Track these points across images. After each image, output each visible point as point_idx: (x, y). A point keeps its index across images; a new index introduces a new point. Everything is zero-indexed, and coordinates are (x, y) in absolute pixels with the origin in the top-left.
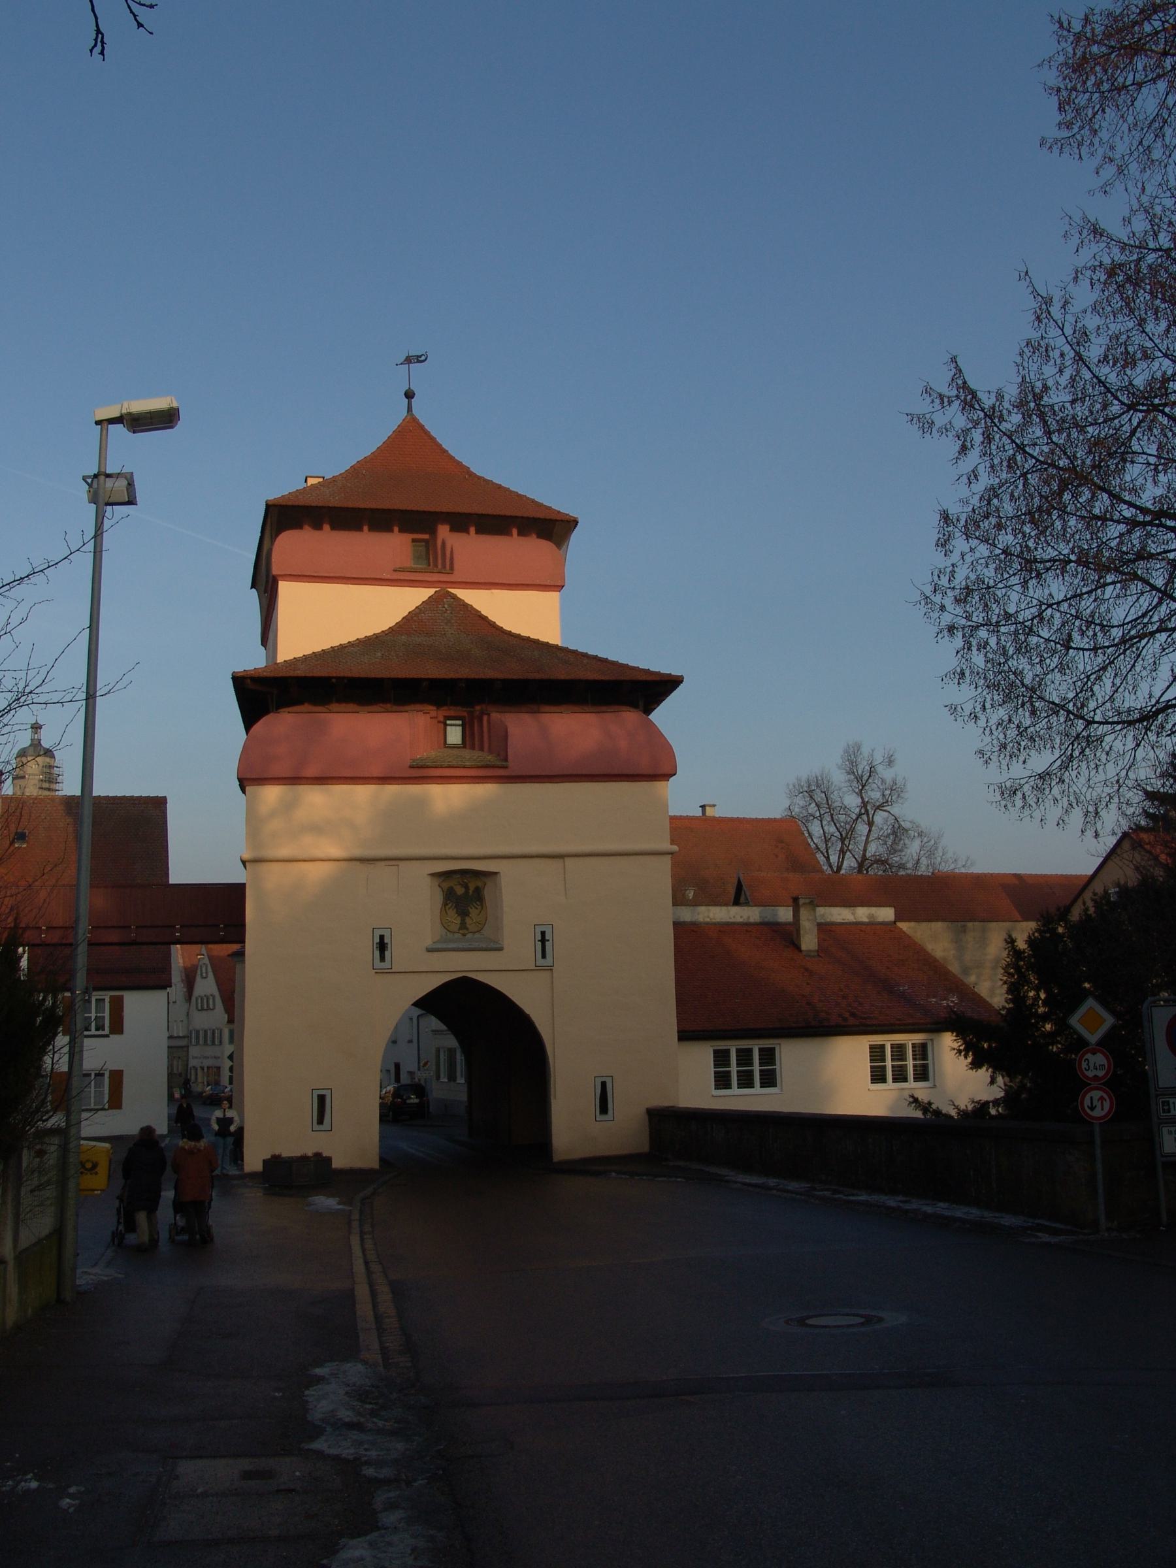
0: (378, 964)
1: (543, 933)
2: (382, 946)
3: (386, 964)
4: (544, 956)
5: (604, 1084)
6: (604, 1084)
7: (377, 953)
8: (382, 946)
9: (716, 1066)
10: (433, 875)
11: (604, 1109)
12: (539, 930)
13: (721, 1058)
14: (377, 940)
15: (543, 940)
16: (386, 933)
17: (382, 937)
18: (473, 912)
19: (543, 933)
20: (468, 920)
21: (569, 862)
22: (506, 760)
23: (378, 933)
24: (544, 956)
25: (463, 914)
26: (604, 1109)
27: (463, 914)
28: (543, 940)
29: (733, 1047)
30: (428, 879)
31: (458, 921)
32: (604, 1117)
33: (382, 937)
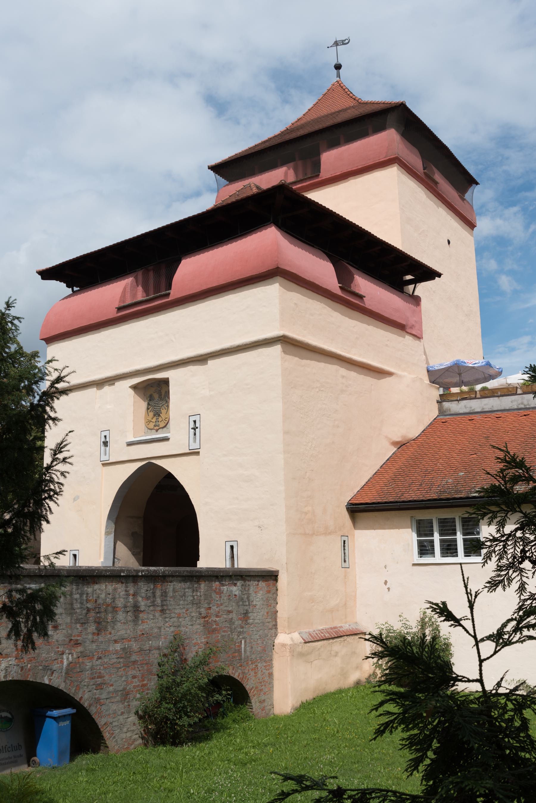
10: (135, 388)
30: (132, 392)
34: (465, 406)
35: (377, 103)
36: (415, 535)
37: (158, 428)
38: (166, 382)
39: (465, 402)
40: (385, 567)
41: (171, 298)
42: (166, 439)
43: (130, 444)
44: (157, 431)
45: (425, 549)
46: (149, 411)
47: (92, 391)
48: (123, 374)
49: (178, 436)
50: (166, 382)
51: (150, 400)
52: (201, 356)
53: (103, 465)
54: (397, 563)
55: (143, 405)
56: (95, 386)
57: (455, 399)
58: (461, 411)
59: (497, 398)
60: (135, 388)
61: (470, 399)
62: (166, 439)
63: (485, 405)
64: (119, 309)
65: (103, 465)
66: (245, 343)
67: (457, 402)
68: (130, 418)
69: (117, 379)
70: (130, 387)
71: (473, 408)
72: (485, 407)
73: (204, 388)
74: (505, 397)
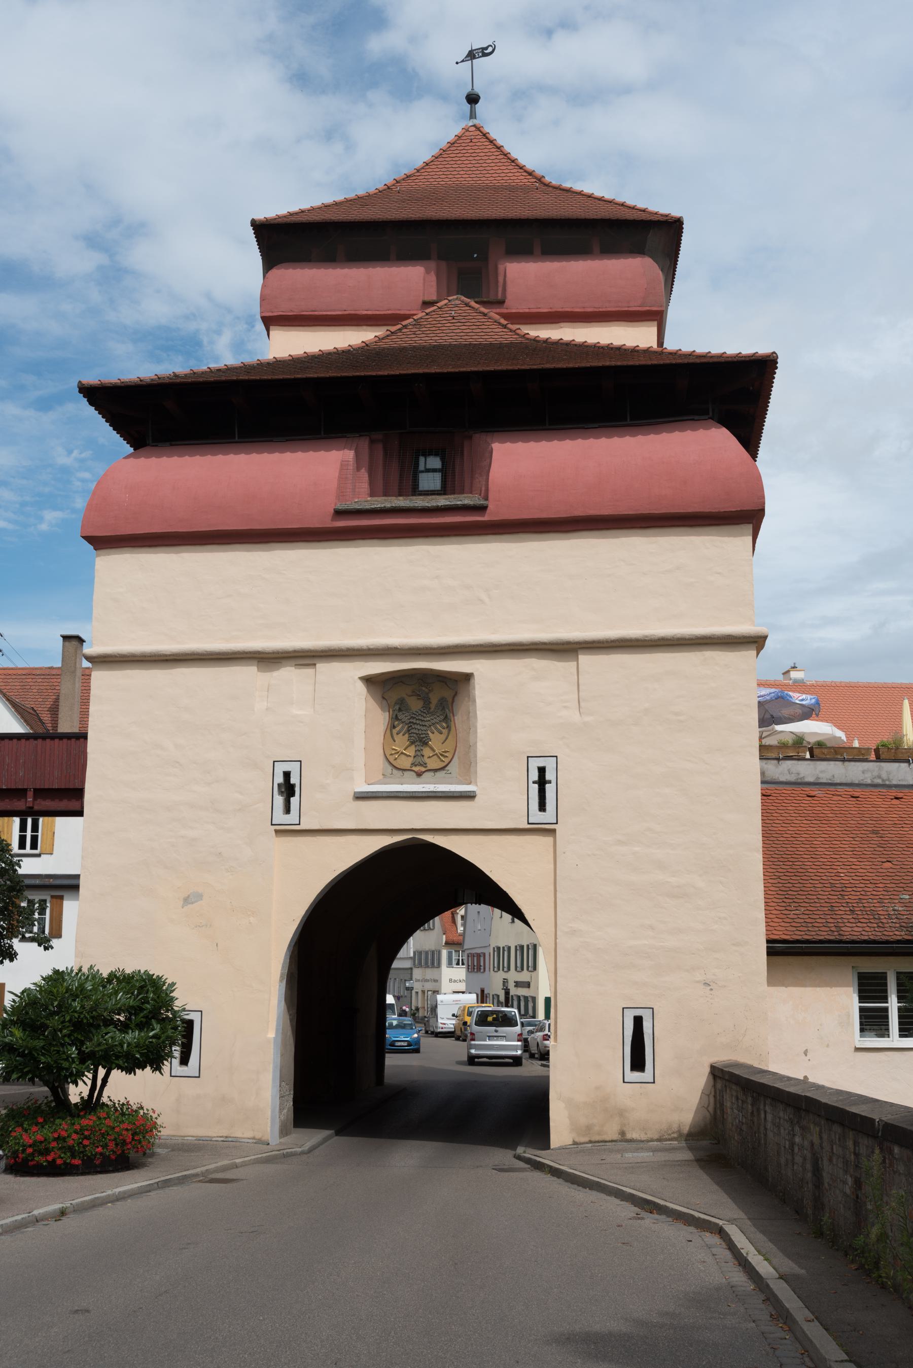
0: (280, 817)
1: (542, 771)
2: (288, 789)
3: (292, 818)
4: (542, 807)
5: (638, 1021)
6: (638, 1021)
7: (279, 800)
8: (288, 789)
9: (862, 999)
10: (369, 681)
11: (638, 1063)
12: (535, 764)
13: (870, 988)
14: (280, 779)
15: (542, 782)
16: (293, 768)
17: (287, 775)
18: (435, 740)
19: (542, 771)
20: (427, 752)
21: (586, 660)
22: (486, 498)
23: (280, 769)
24: (542, 807)
25: (421, 741)
26: (638, 1063)
27: (421, 741)
28: (542, 782)
29: (891, 970)
30: (361, 688)
31: (411, 751)
32: (637, 1076)
33: (287, 775)
34: (789, 771)
35: (629, 207)
36: (856, 998)
37: (423, 769)
38: (460, 683)
39: (789, 763)
40: (806, 1053)
41: (486, 518)
42: (469, 796)
43: (361, 797)
44: (419, 775)
45: (873, 1022)
46: (395, 731)
47: (248, 673)
48: (348, 650)
49: (500, 794)
50: (460, 683)
51: (400, 710)
52: (568, 643)
53: (277, 831)
54: (828, 1046)
55: (381, 719)
56: (255, 662)
57: (774, 756)
58: (782, 779)
59: (839, 763)
60: (369, 681)
61: (798, 760)
62: (469, 796)
63: (821, 772)
64: (339, 513)
65: (277, 831)
66: (679, 636)
67: (776, 762)
68: (360, 741)
69: (321, 656)
70: (361, 678)
71: (801, 776)
72: (821, 775)
73: (565, 707)
74: (853, 763)
